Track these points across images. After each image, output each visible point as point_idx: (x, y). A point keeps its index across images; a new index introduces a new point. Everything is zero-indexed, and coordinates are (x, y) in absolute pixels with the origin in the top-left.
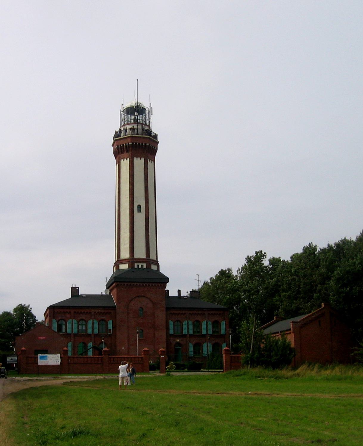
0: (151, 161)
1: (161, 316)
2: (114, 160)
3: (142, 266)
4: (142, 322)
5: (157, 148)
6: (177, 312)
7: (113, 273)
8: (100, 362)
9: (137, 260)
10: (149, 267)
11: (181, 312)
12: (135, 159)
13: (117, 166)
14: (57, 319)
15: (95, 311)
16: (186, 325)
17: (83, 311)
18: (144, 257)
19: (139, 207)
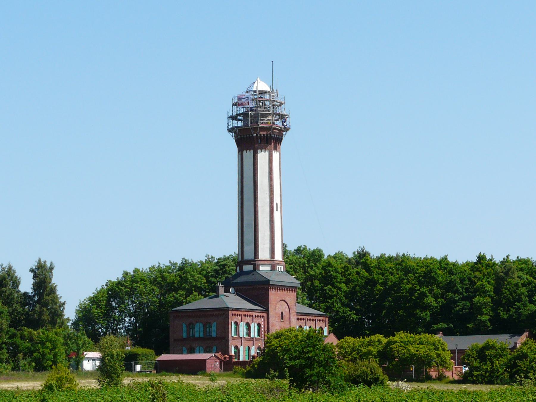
3: (281, 268)
9: (277, 262)
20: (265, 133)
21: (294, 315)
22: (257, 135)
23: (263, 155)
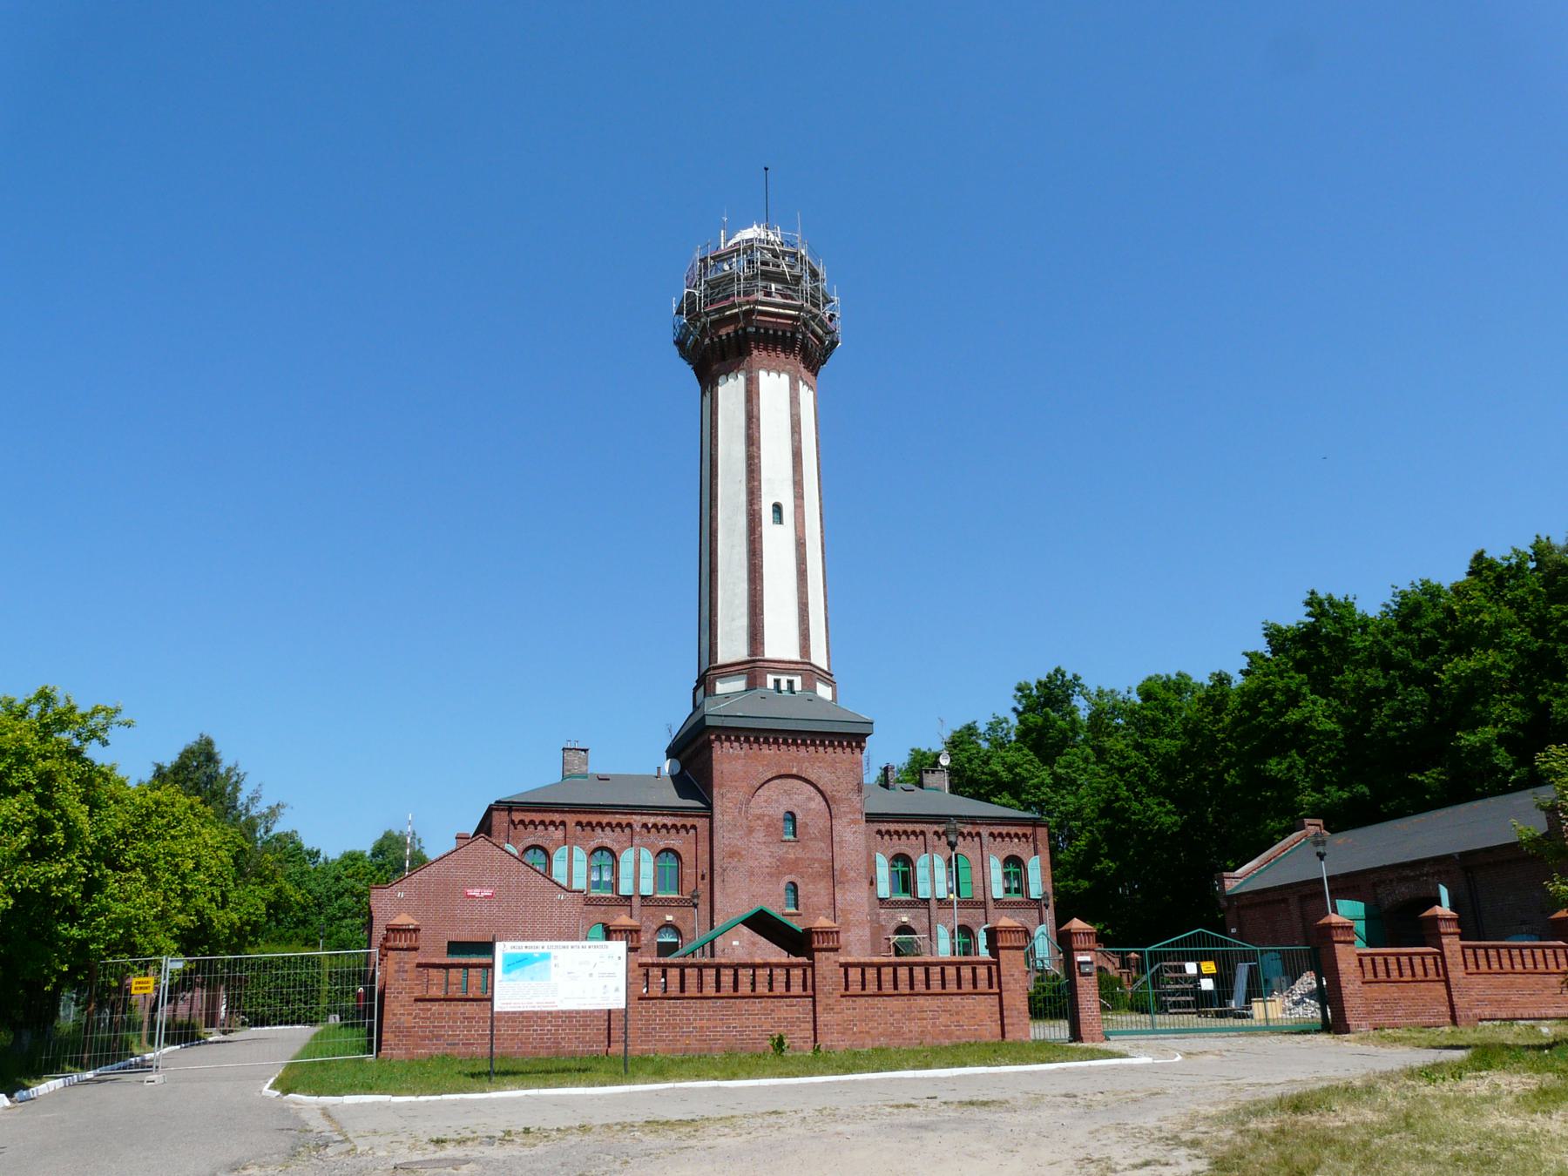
0: (806, 388)
1: (852, 836)
2: (698, 388)
3: (790, 683)
4: (792, 856)
6: (900, 827)
8: (796, 989)
9: (772, 665)
10: (809, 686)
11: (910, 827)
12: (762, 374)
14: (521, 846)
15: (645, 819)
16: (927, 870)
17: (605, 819)
18: (796, 657)
19: (777, 508)
20: (730, 329)
21: (854, 822)
22: (711, 339)
23: (733, 386)
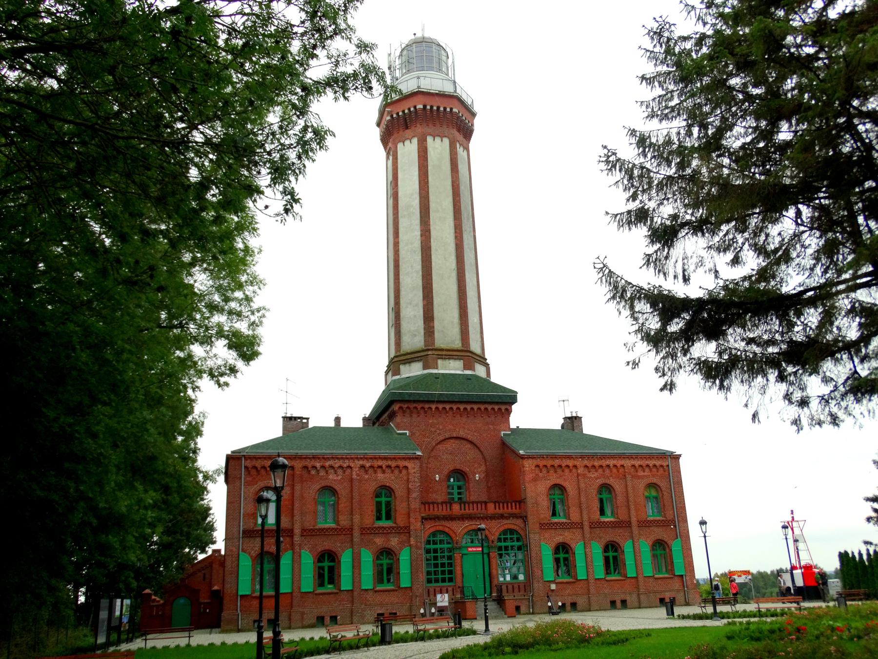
5: (472, 125)
7: (382, 387)
12: (429, 139)
13: (390, 162)
18: (458, 344)
